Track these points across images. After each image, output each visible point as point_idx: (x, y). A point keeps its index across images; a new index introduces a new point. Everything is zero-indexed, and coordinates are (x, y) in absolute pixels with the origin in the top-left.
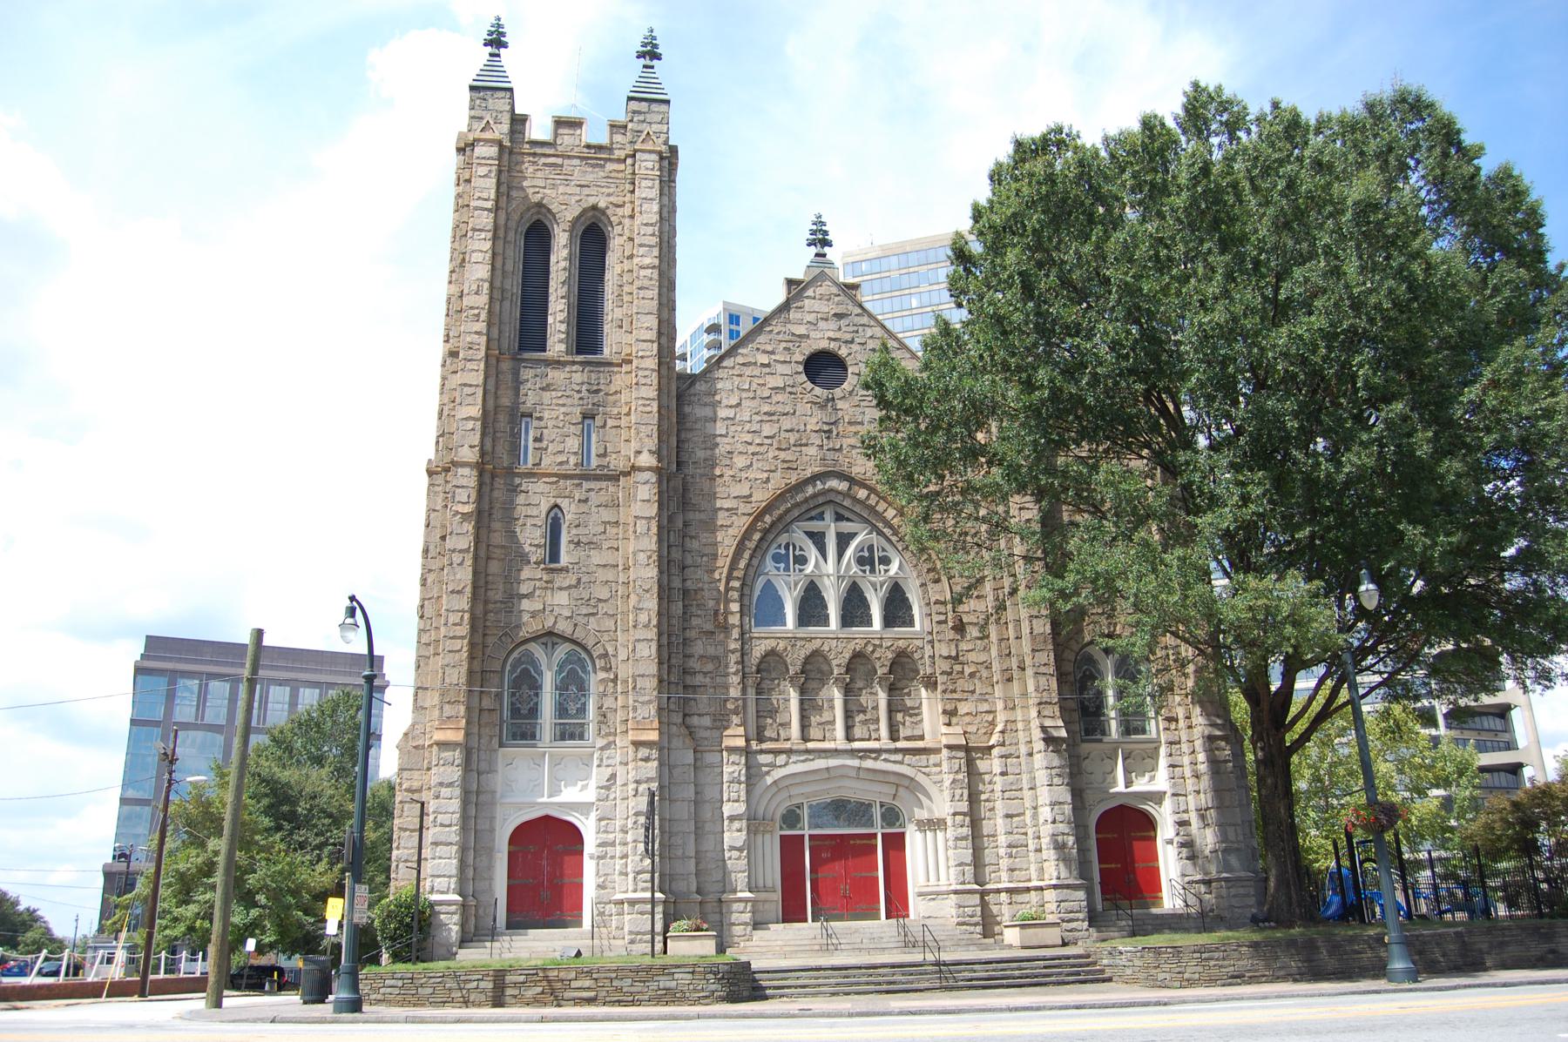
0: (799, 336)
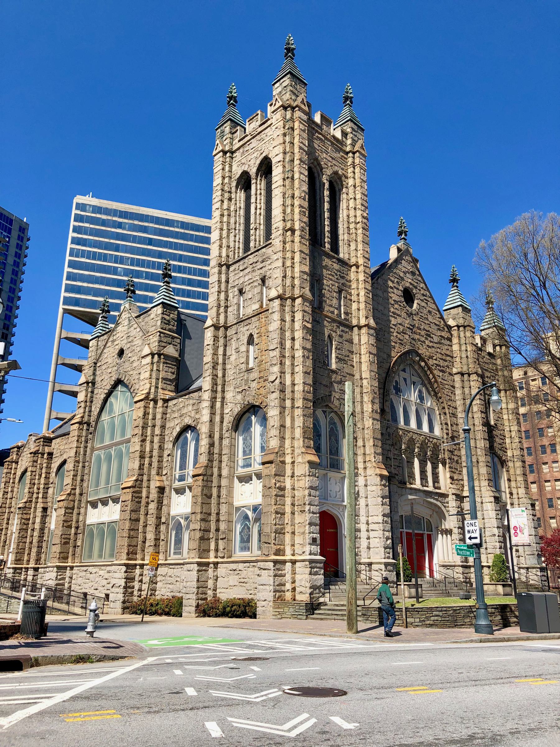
0: (401, 277)
